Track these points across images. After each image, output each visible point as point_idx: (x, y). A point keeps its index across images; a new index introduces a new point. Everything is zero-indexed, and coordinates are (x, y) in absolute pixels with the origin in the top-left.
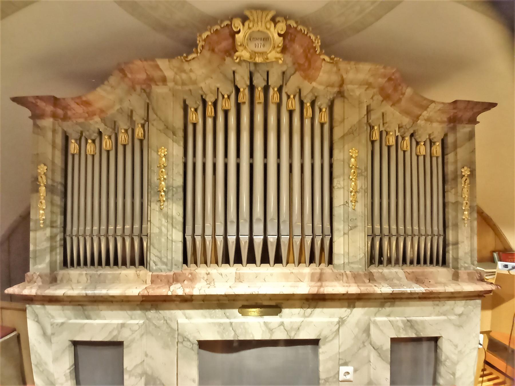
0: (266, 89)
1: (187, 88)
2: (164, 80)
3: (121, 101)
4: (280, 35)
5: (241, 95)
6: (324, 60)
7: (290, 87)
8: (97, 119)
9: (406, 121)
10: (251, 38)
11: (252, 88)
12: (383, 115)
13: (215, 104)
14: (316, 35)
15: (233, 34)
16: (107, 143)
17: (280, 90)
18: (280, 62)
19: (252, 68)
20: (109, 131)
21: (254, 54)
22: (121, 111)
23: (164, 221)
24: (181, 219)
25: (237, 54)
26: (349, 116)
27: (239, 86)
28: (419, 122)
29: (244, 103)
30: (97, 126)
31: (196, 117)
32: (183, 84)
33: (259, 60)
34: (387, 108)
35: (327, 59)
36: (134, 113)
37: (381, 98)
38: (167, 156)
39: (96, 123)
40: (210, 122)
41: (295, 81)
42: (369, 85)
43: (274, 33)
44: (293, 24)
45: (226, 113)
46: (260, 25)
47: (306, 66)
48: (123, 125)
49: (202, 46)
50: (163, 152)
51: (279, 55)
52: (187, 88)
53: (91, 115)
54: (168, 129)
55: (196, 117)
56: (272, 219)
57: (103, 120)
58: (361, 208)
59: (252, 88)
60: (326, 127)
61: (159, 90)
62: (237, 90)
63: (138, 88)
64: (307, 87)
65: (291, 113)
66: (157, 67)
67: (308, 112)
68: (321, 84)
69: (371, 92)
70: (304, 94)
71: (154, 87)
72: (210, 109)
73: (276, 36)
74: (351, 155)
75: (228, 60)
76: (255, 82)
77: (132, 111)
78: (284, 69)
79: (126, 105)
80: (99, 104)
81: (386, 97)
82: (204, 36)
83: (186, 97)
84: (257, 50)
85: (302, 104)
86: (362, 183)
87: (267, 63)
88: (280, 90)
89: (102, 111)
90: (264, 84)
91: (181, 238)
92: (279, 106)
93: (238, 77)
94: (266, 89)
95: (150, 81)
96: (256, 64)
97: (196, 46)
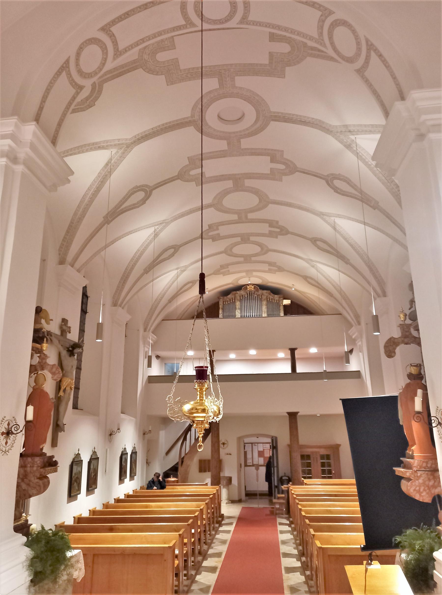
7: (255, 293)
16: (229, 302)
26: (264, 297)
31: (241, 298)
39: (228, 299)
43: (253, 287)
47: (257, 291)
54: (238, 300)
55: (241, 298)
58: (266, 310)
61: (237, 295)
64: (258, 293)
74: (264, 303)
86: (266, 307)
87: (252, 291)
95: (235, 294)
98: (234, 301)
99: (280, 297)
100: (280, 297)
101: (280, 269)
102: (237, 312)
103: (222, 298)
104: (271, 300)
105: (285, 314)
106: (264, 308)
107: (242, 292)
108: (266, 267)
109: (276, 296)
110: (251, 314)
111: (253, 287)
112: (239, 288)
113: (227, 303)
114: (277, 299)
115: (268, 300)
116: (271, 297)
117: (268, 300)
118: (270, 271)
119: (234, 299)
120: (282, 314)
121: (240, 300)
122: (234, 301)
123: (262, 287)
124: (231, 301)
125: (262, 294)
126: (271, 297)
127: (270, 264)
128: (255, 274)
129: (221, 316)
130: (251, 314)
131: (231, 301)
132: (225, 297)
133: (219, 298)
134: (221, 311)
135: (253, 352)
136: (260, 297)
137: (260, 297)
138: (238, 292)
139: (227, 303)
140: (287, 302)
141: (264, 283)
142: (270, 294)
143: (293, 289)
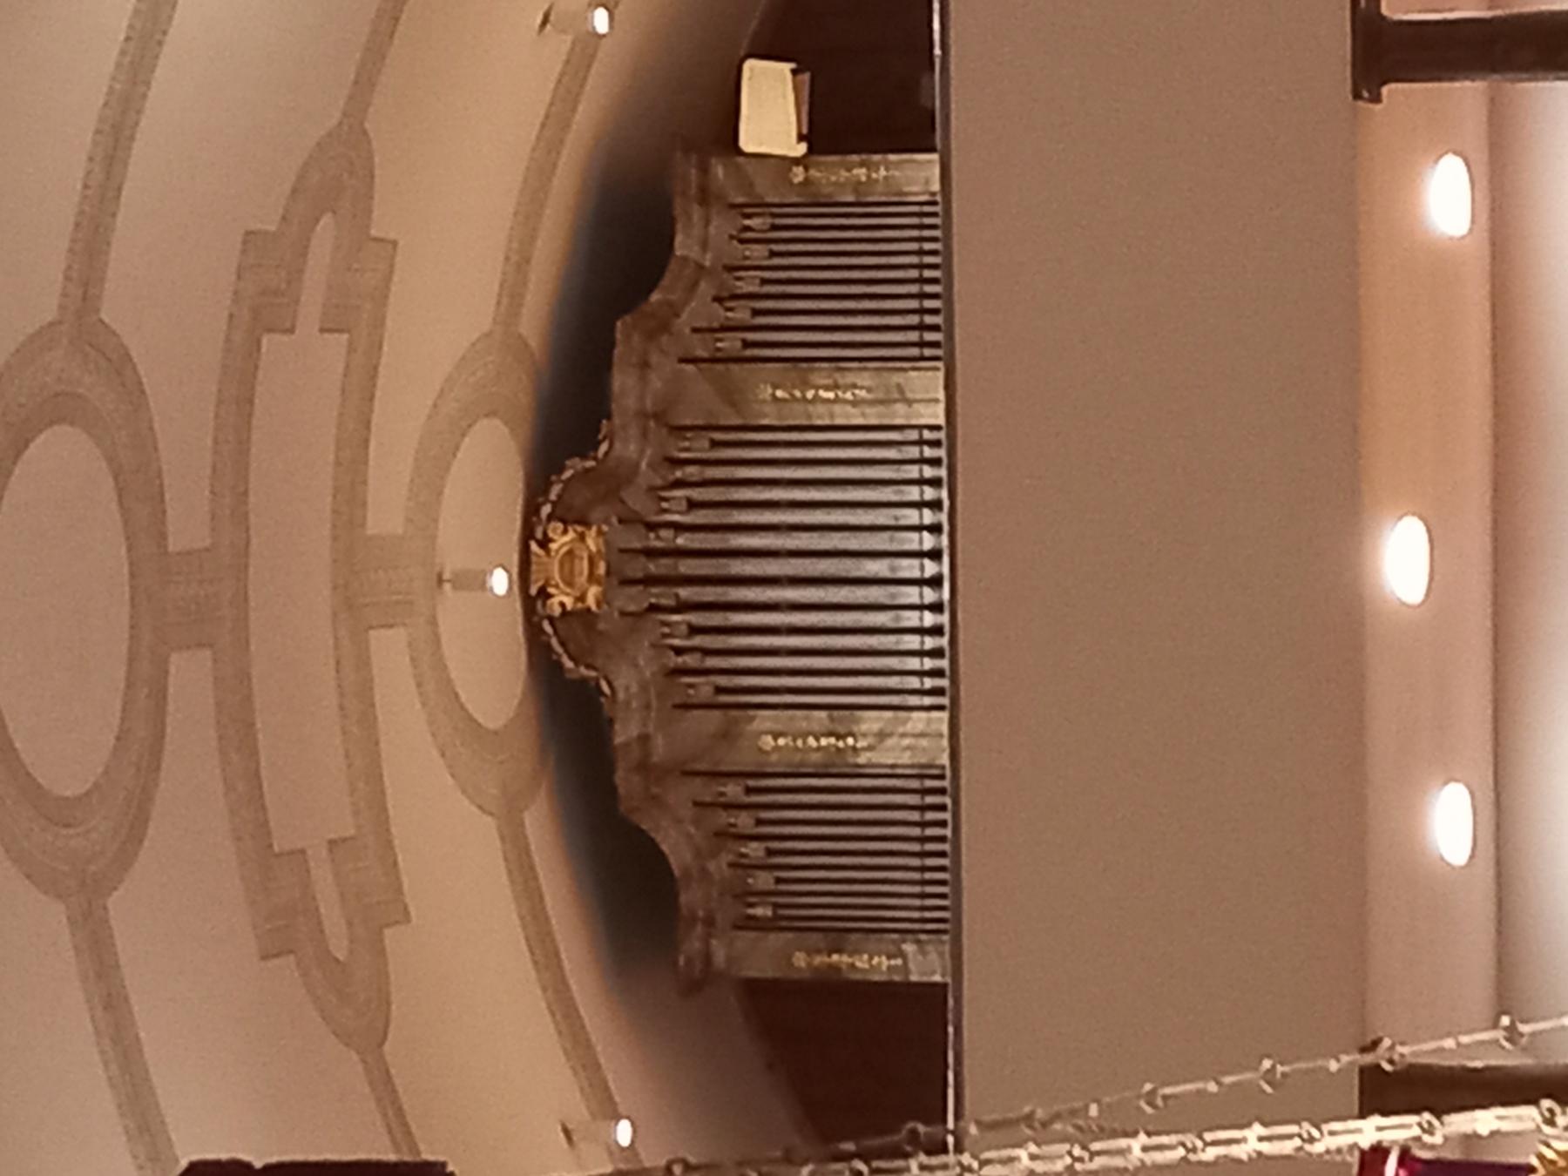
0: (651, 553)
1: (654, 703)
2: (644, 739)
3: (679, 821)
4: (565, 532)
5: (664, 602)
6: (606, 454)
8: (712, 866)
9: (706, 288)
10: (570, 584)
11: (649, 581)
12: (695, 330)
13: (679, 651)
14: (562, 469)
15: (565, 613)
16: (755, 850)
17: (652, 527)
18: (605, 528)
19: (615, 582)
20: (731, 844)
21: (592, 578)
22: (697, 822)
23: (890, 742)
24: (889, 714)
25: (594, 608)
26: (700, 398)
27: (646, 605)
28: (707, 264)
29: (677, 596)
30: (724, 866)
32: (648, 707)
33: (601, 569)
34: (684, 322)
35: (604, 447)
36: (699, 799)
37: (664, 339)
38: (772, 737)
39: (719, 866)
40: (712, 662)
41: (635, 500)
42: (645, 365)
43: (562, 540)
44: (546, 510)
45: (694, 630)
46: (549, 567)
48: (724, 818)
49: (588, 666)
50: (768, 742)
51: (594, 529)
52: (654, 703)
53: (704, 871)
54: (727, 735)
55: (703, 688)
56: (892, 540)
57: (714, 855)
59: (649, 581)
60: (719, 436)
61: (660, 748)
62: (654, 608)
63: (655, 790)
65: (693, 505)
66: (626, 745)
67: (692, 471)
68: (642, 452)
69: (654, 359)
70: (659, 482)
71: (655, 759)
72: (690, 660)
73: (567, 538)
74: (769, 395)
75: (601, 626)
76: (640, 575)
77: (696, 804)
78: (614, 520)
79: (687, 812)
80: (688, 857)
81: (664, 327)
82: (569, 664)
83: (669, 704)
84: (586, 572)
85: (679, 484)
87: (617, 555)
88: (652, 527)
89: (698, 854)
90: (643, 559)
91: (923, 715)
92: (679, 528)
93: (632, 608)
94: (651, 553)
95: (643, 766)
96: (608, 573)
97: (584, 681)
98: (733, 790)
99: (705, 196)
100: (705, 196)
101: (340, 176)
102: (885, 756)
103: (693, 945)
104: (741, 314)
105: (916, 130)
106: (845, 399)
107: (627, 680)
108: (303, 365)
109: (684, 245)
110: (909, 568)
111: (562, 540)
112: (570, 712)
113: (764, 880)
114: (721, 226)
115: (730, 343)
116: (700, 309)
117: (730, 343)
118: (359, 316)
119: (699, 789)
120: (917, 174)
121: (734, 703)
122: (733, 790)
123: (569, 423)
124: (744, 821)
125: (662, 419)
126: (700, 309)
127: (263, 310)
128: (386, 513)
129: (923, 964)
130: (909, 568)
131: (744, 821)
132: (690, 898)
133: (698, 982)
134: (871, 963)
135: (1402, 561)
136: (700, 447)
137: (700, 447)
138: (624, 733)
139: (764, 880)
140: (770, 110)
141: (520, 392)
142: (662, 326)
143: (601, 21)
